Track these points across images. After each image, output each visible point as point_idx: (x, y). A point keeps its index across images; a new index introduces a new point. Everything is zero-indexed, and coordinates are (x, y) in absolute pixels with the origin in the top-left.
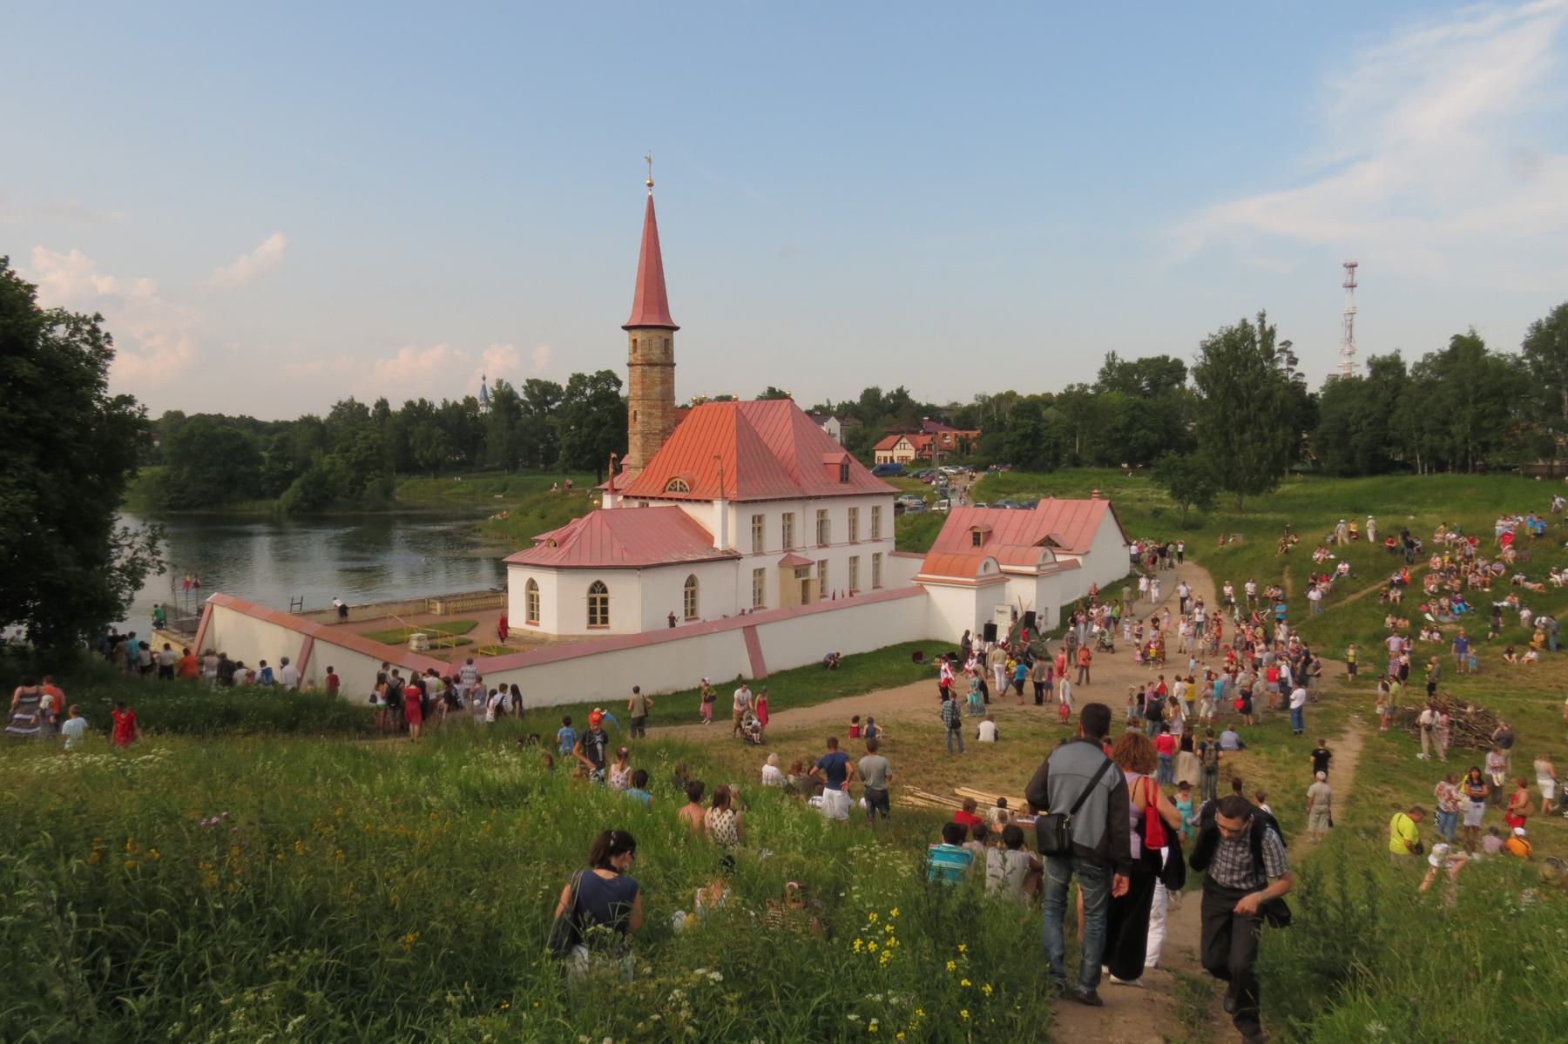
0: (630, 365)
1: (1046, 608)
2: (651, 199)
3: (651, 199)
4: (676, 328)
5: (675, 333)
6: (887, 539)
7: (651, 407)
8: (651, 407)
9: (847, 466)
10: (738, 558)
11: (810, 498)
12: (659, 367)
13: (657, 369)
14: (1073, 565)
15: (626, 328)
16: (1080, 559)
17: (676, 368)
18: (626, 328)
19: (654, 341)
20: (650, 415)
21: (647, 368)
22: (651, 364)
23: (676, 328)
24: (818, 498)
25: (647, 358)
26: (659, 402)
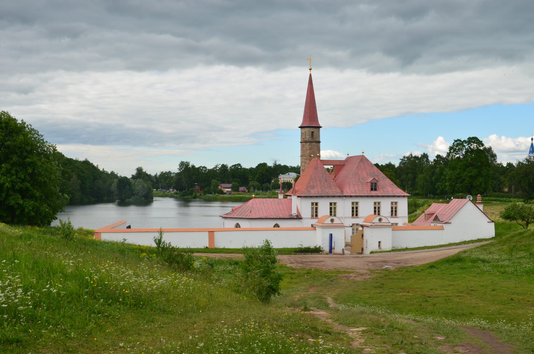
0: (301, 142)
1: (379, 242)
2: (310, 75)
3: (310, 75)
4: (321, 127)
5: (320, 128)
9: (376, 184)
10: (301, 218)
11: (345, 196)
12: (308, 143)
13: (308, 144)
14: (442, 228)
15: (299, 127)
16: (444, 225)
18: (299, 127)
19: (307, 132)
20: (305, 162)
21: (304, 144)
22: (306, 142)
23: (321, 127)
24: (351, 196)
25: (305, 139)
26: (309, 157)
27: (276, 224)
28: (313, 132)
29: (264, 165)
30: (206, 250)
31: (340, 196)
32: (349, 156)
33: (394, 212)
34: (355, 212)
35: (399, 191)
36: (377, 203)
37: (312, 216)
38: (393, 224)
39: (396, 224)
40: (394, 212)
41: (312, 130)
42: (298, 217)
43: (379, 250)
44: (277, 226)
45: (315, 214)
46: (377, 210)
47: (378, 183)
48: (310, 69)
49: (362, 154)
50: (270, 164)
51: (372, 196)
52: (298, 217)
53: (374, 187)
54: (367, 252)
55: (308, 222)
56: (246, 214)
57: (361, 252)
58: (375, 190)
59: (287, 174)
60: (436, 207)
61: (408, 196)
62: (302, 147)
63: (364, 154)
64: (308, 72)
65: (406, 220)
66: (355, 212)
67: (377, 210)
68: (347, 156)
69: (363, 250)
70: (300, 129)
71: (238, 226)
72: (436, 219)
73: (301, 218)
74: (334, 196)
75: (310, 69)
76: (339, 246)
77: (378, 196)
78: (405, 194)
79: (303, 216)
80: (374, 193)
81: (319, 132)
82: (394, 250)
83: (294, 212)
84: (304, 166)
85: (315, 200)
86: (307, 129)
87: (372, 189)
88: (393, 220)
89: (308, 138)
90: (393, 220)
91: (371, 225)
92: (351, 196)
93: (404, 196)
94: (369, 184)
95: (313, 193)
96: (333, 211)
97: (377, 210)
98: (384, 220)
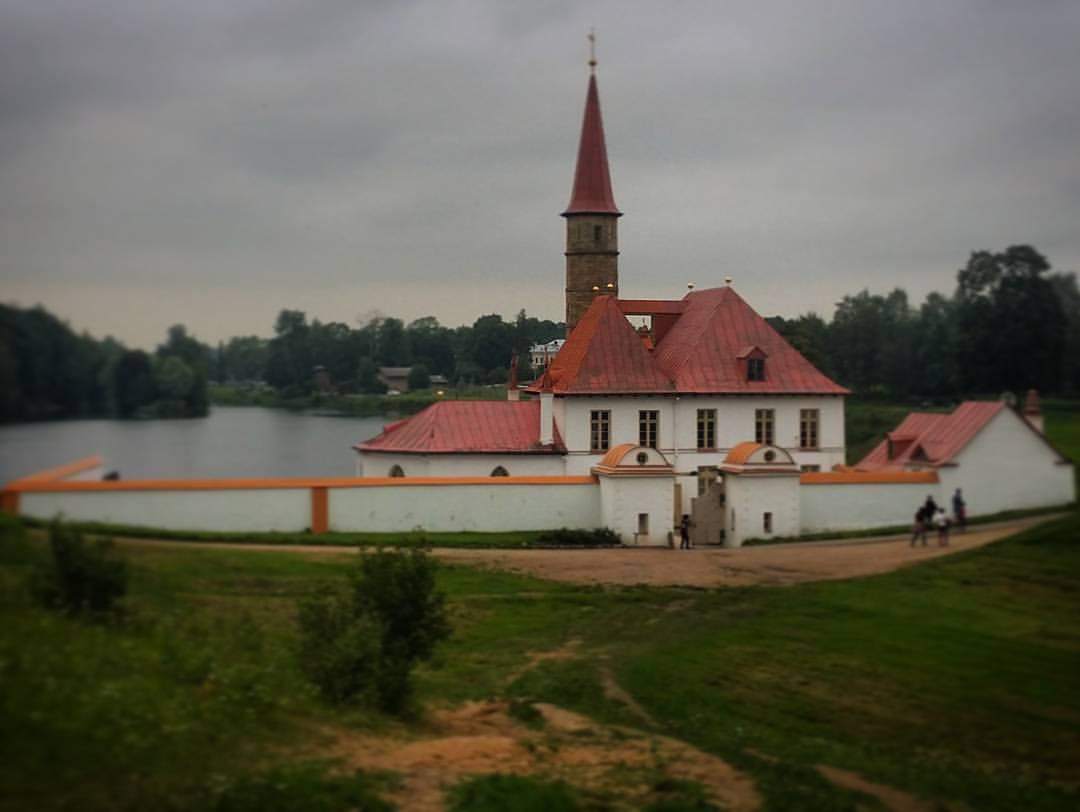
0: (567, 254)
1: (767, 516)
4: (620, 215)
5: (619, 219)
6: (830, 450)
7: (579, 299)
8: (579, 299)
9: (761, 363)
10: (565, 453)
11: (680, 395)
13: (585, 258)
15: (564, 215)
17: (619, 257)
18: (564, 215)
21: (576, 258)
23: (620, 215)
24: (695, 395)
27: (500, 468)
28: (598, 229)
29: (496, 318)
30: (306, 538)
31: (666, 395)
32: (693, 290)
33: (809, 438)
34: (706, 438)
35: (821, 382)
36: (648, 415)
37: (595, 446)
38: (805, 468)
39: (815, 468)
40: (809, 438)
41: (594, 222)
42: (558, 451)
43: (767, 537)
44: (500, 472)
45: (601, 440)
46: (764, 431)
47: (767, 361)
48: (593, 64)
49: (726, 285)
50: (509, 318)
51: (751, 396)
52: (558, 451)
53: (755, 368)
54: (737, 538)
55: (582, 464)
56: (420, 442)
57: (717, 541)
58: (761, 378)
59: (553, 343)
60: (917, 425)
61: (844, 395)
62: (571, 266)
63: (731, 285)
64: (587, 72)
65: (840, 459)
66: (706, 438)
67: (764, 431)
68: (689, 291)
69: (723, 534)
70: (565, 219)
71: (397, 472)
72: (919, 454)
73: (565, 453)
74: (650, 395)
75: (593, 64)
76: (662, 525)
77: (766, 395)
78: (839, 389)
79: (569, 447)
80: (755, 387)
81: (614, 228)
82: (806, 538)
83: (546, 438)
84: (576, 316)
85: (601, 407)
86: (582, 221)
87: (751, 377)
88: (803, 459)
89: (587, 243)
90: (803, 459)
91: (745, 471)
92: (695, 395)
93: (835, 395)
94: (745, 364)
95: (596, 384)
96: (649, 433)
97: (764, 430)
98: (780, 457)
